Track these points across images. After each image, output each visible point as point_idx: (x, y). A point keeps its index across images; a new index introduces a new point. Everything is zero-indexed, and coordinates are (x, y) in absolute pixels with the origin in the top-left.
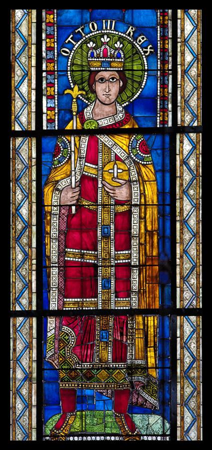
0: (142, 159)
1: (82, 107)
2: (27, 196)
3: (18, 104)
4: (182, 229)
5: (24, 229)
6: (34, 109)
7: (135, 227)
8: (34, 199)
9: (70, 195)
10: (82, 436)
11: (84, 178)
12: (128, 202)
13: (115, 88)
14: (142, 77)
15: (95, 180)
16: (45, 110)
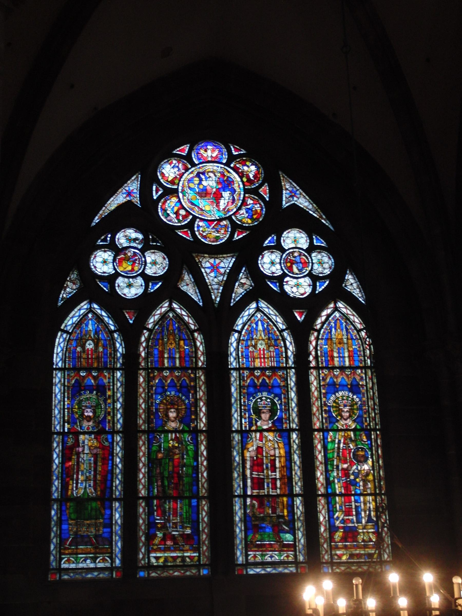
0: (279, 440)
1: (256, 422)
2: (238, 453)
3: (234, 421)
7: (278, 464)
8: (240, 454)
9: (254, 453)
12: (274, 456)
15: (262, 448)
16: (243, 423)
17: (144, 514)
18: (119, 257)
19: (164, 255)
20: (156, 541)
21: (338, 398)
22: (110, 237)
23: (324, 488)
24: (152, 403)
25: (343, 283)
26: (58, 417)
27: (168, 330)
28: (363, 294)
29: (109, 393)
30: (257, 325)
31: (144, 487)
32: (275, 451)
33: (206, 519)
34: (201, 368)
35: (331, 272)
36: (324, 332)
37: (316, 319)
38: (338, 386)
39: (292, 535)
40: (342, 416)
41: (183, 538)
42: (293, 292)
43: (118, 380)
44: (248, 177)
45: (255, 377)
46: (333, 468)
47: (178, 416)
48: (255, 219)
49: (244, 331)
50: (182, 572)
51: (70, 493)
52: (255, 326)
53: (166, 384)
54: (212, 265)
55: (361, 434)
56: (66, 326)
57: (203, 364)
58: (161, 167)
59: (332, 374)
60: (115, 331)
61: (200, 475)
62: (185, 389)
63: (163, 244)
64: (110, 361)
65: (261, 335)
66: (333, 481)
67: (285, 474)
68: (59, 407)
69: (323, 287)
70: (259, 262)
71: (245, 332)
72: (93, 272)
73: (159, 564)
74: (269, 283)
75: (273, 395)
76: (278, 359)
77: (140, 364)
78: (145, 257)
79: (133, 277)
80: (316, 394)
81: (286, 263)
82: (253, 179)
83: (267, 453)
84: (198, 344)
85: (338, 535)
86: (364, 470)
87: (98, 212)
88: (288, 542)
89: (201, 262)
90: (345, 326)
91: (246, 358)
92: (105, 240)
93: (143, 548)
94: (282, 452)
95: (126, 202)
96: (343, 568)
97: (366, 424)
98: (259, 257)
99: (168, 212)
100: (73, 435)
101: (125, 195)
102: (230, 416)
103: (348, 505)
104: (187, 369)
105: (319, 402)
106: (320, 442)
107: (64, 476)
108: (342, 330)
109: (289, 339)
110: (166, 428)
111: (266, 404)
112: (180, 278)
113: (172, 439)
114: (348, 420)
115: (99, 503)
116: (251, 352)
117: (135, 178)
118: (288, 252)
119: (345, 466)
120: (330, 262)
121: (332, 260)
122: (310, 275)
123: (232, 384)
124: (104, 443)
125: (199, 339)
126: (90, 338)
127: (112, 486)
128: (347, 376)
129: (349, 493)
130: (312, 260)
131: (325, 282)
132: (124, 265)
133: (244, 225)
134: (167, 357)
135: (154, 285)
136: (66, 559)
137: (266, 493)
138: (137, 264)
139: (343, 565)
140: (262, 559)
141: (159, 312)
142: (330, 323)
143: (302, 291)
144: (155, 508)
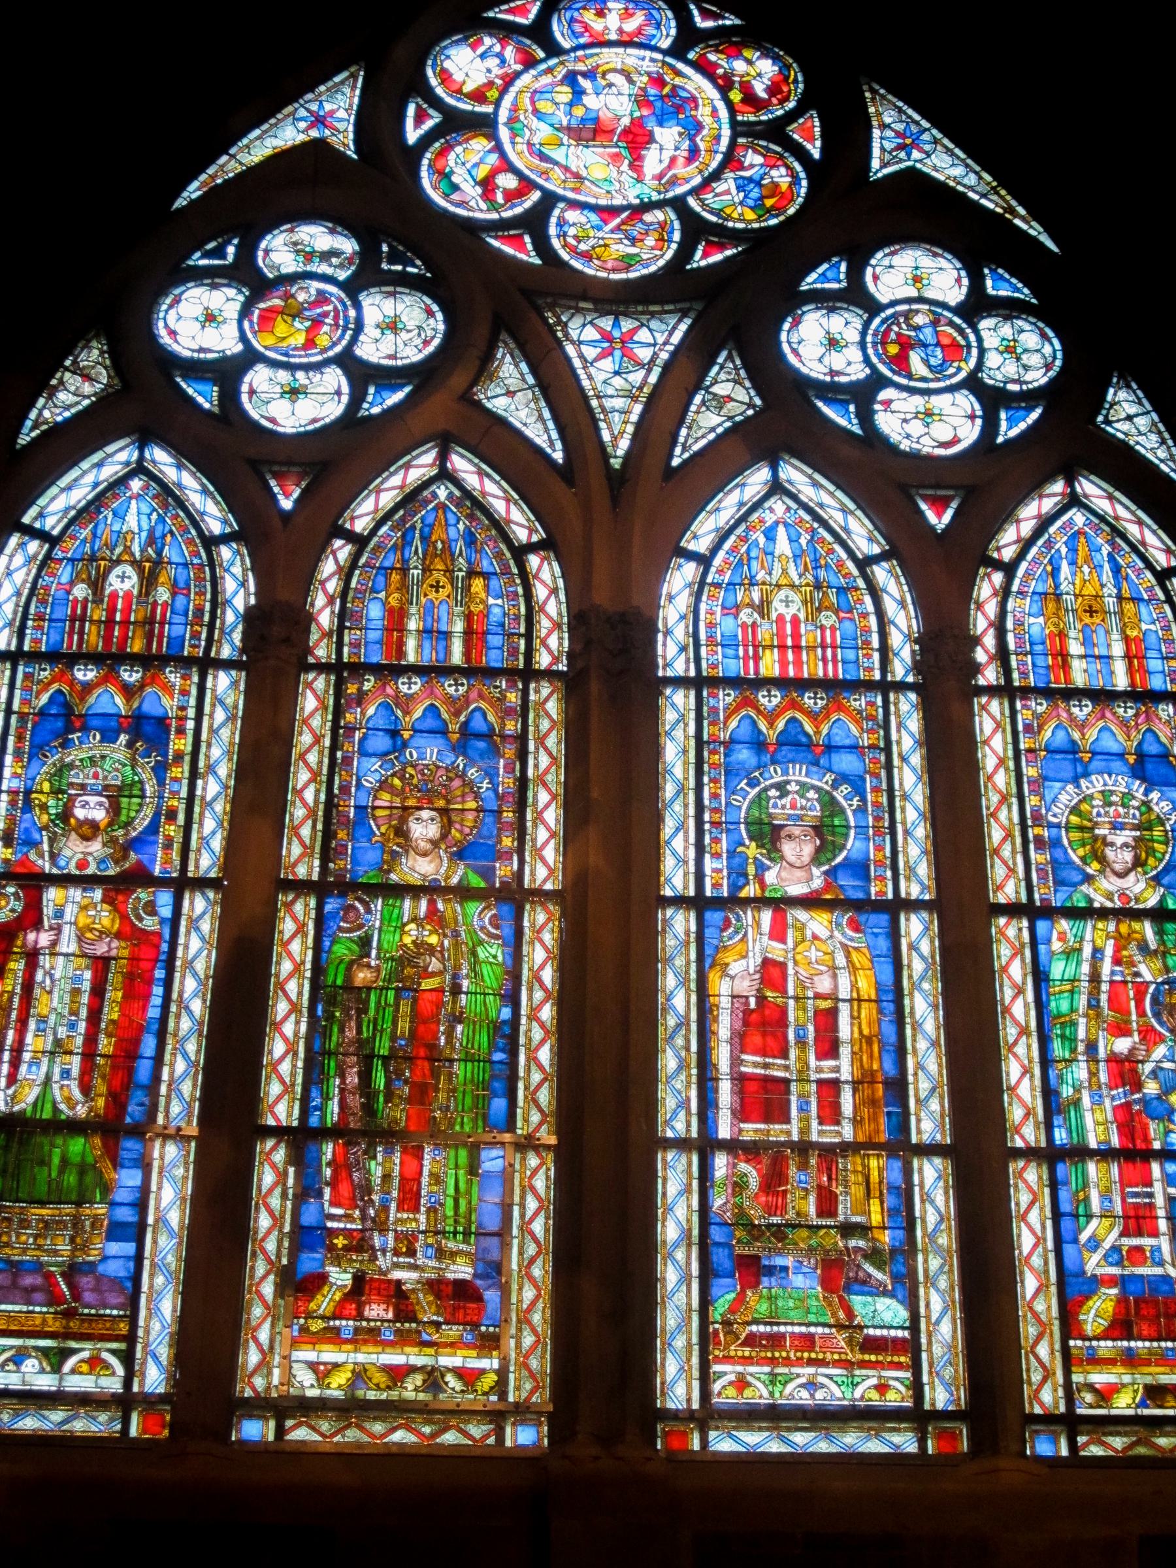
0: (852, 940)
1: (761, 869)
2: (685, 982)
3: (668, 863)
4: (914, 1036)
5: (678, 1026)
6: (692, 868)
7: (845, 1030)
8: (693, 986)
9: (746, 983)
10: (771, 1324)
11: (767, 963)
13: (808, 850)
14: (846, 836)
15: (783, 966)
16: (708, 870)
17: (278, 1191)
18: (262, 305)
19: (428, 301)
20: (324, 1302)
21: (1091, 797)
22: (237, 247)
23: (1037, 1125)
24: (345, 789)
25: (1099, 413)
27: (424, 539)
29: (183, 744)
30: (770, 535)
31: (288, 1089)
33: (538, 1227)
34: (549, 674)
35: (1052, 381)
36: (1027, 573)
39: (901, 1302)
41: (438, 1296)
42: (908, 436)
43: (218, 700)
44: (747, 89)
45: (759, 712)
46: (1073, 1050)
47: (444, 835)
48: (768, 211)
50: (427, 1430)
52: (762, 540)
53: (407, 721)
56: (41, 515)
57: (556, 660)
58: (441, 52)
59: (1064, 715)
60: (225, 539)
61: (522, 1058)
62: (482, 744)
63: (428, 270)
64: (196, 635)
65: (785, 572)
66: (1077, 1103)
67: (875, 1067)
69: (1023, 426)
70: (783, 336)
72: (162, 349)
73: (328, 1392)
74: (820, 404)
75: (829, 777)
76: (850, 655)
77: (309, 651)
78: (358, 306)
79: (307, 368)
80: (1000, 779)
81: (884, 343)
82: (764, 95)
83: (801, 984)
84: (541, 592)
87: (203, 171)
88: (885, 1332)
89: (565, 326)
90: (1109, 554)
92: (219, 252)
93: (267, 1326)
94: (866, 987)
95: (304, 144)
96: (1118, 1442)
98: (783, 320)
99: (455, 179)
100: (21, 887)
101: (303, 125)
103: (1136, 1195)
104: (492, 673)
105: (1015, 808)
106: (1018, 952)
108: (1098, 568)
109: (892, 588)
110: (393, 876)
111: (802, 808)
112: (484, 369)
113: (414, 919)
114: (1132, 877)
115: (98, 1141)
116: (744, 626)
117: (347, 79)
118: (889, 311)
119: (1122, 1045)
120: (1047, 350)
121: (1056, 342)
122: (973, 384)
123: (667, 734)
124: (141, 919)
125: (545, 575)
126: (126, 557)
127: (156, 1078)
128: (1124, 723)
129: (1140, 1145)
130: (980, 340)
131: (1030, 409)
132: (281, 328)
133: (730, 224)
134: (418, 631)
135: (385, 394)
138: (326, 328)
139: (1121, 1429)
140: (771, 1394)
141: (396, 480)
142: (1049, 544)
143: (943, 432)
144: (328, 1172)
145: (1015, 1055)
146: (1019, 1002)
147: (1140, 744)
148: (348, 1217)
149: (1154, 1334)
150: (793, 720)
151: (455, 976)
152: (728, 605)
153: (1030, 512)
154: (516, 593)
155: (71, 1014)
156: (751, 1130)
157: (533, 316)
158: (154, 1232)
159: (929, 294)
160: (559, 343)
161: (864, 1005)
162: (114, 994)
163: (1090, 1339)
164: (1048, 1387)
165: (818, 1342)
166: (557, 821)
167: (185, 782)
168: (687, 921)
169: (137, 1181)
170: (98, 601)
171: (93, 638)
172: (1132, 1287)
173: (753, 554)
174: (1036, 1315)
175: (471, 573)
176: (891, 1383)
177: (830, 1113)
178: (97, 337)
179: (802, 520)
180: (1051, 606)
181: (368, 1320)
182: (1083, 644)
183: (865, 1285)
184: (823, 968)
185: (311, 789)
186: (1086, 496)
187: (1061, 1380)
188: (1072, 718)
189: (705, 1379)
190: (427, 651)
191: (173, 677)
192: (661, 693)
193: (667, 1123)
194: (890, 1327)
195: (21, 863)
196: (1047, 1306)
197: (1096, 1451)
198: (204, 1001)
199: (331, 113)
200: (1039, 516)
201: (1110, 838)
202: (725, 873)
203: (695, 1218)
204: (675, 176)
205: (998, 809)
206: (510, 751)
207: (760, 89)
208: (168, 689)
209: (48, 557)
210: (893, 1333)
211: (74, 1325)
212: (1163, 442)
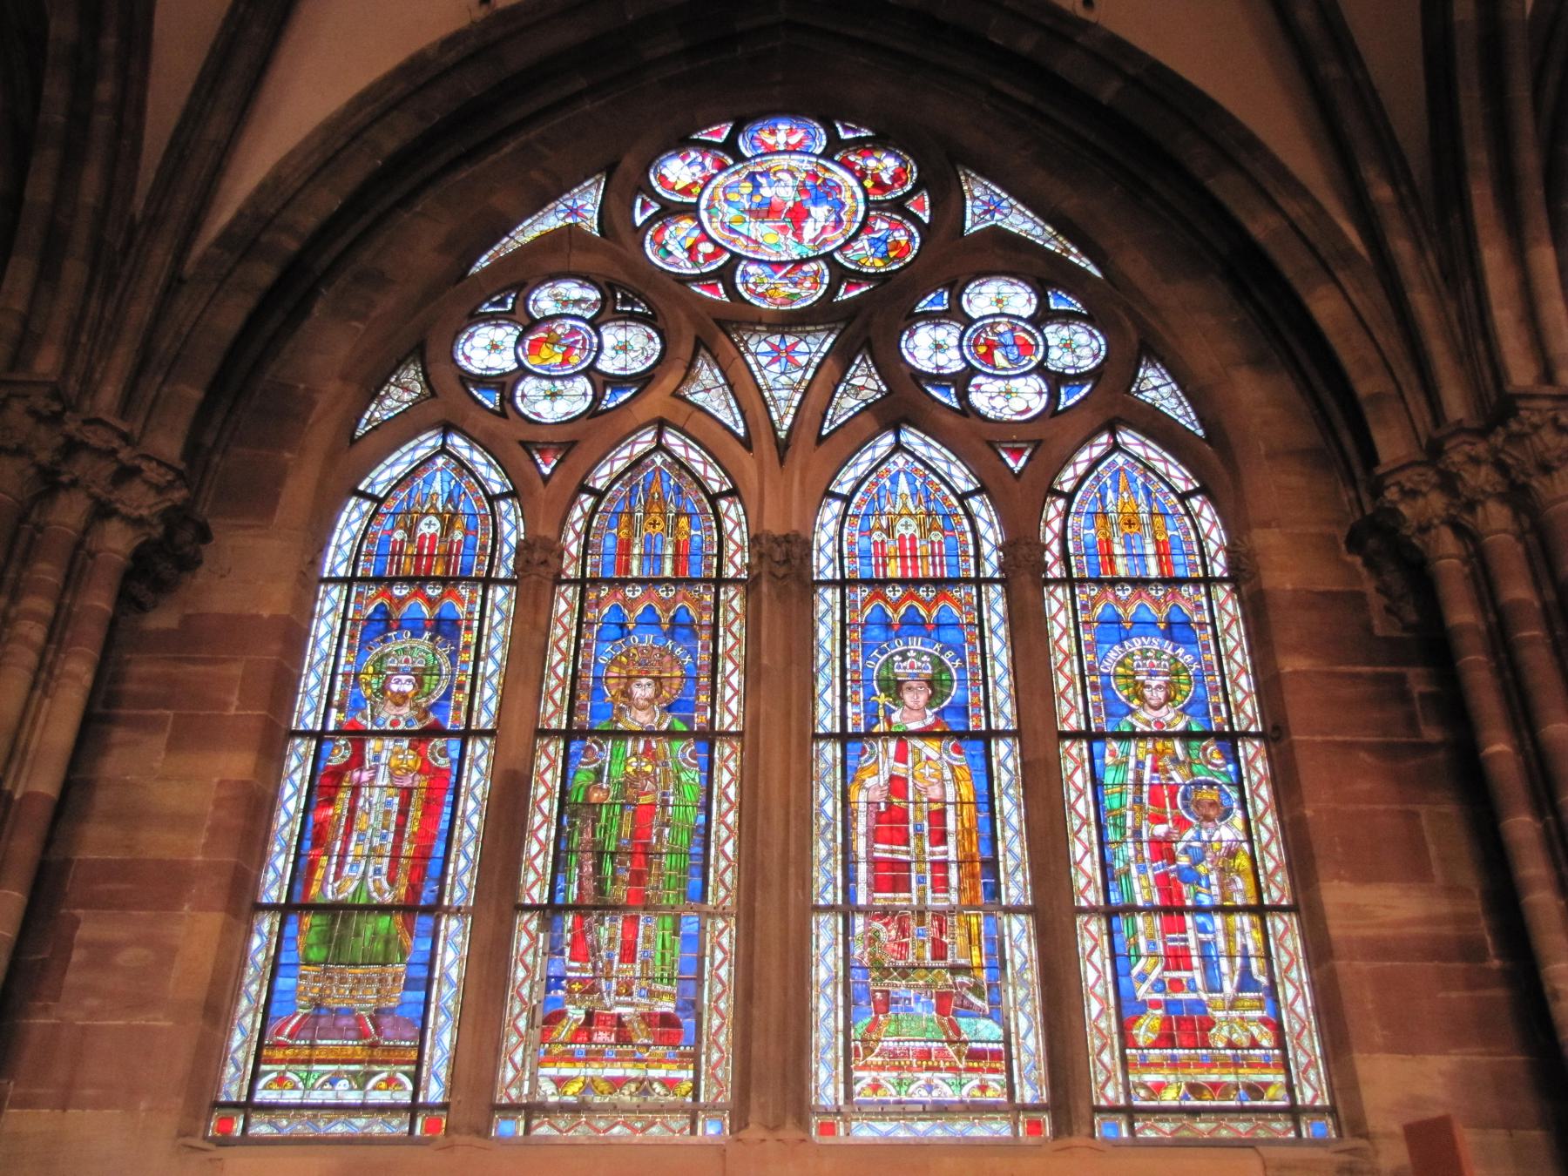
1: (889, 712)
3: (821, 710)
5: (828, 825)
6: (838, 713)
7: (951, 824)
8: (839, 796)
9: (878, 793)
11: (893, 778)
13: (923, 698)
15: (905, 780)
17: (531, 951)
18: (532, 338)
19: (650, 330)
20: (563, 1031)
21: (1132, 654)
26: (316, 693)
28: (1189, 409)
30: (894, 480)
32: (943, 787)
33: (723, 972)
34: (734, 581)
36: (1082, 501)
37: (1061, 468)
38: (1128, 626)
40: (1142, 698)
41: (649, 1025)
42: (994, 408)
43: (496, 606)
45: (886, 602)
46: (1123, 835)
47: (657, 696)
48: (892, 260)
49: (858, 495)
51: (315, 889)
52: (888, 484)
54: (775, 348)
55: (1205, 749)
56: (372, 484)
57: (739, 571)
59: (1111, 597)
60: (503, 496)
62: (686, 631)
63: (649, 309)
64: (481, 563)
65: (905, 505)
66: (1127, 873)
68: (320, 670)
69: (1077, 397)
70: (903, 344)
71: (862, 500)
73: (565, 1098)
76: (953, 560)
77: (561, 571)
78: (599, 334)
79: (562, 378)
81: (975, 345)
82: (889, 182)
84: (729, 525)
85: (1146, 1028)
86: (1221, 841)
89: (746, 343)
91: (861, 557)
92: (502, 303)
93: (520, 1050)
97: (1218, 720)
98: (902, 333)
99: (669, 248)
100: (350, 740)
101: (561, 215)
102: (809, 696)
104: (691, 582)
105: (1076, 663)
107: (307, 844)
109: (984, 513)
113: (634, 754)
114: (1164, 709)
115: (399, 918)
116: (876, 543)
118: (979, 324)
119: (1160, 830)
120: (1095, 344)
122: (1041, 370)
123: (820, 620)
125: (732, 513)
127: (444, 873)
128: (1155, 601)
130: (1045, 340)
131: (1082, 386)
132: (545, 352)
133: (865, 270)
136: (274, 1075)
137: (915, 902)
138: (577, 351)
140: (899, 1093)
141: (626, 453)
142: (1098, 478)
144: (569, 937)
145: (1079, 839)
146: (1082, 801)
147: (1168, 615)
148: (584, 969)
149: (1193, 1045)
150: (911, 607)
151: (664, 794)
152: (864, 529)
153: (1083, 458)
154: (711, 527)
155: (383, 828)
156: (882, 898)
157: (722, 337)
158: (439, 983)
159: (1008, 311)
160: (742, 354)
161: (965, 806)
162: (415, 813)
163: (1142, 1049)
164: (1110, 1086)
165: (934, 1053)
166: (739, 683)
167: (471, 664)
168: (834, 750)
169: (428, 947)
170: (411, 541)
171: (407, 566)
172: (1172, 1008)
173: (882, 494)
174: (1099, 1030)
175: (678, 515)
176: (990, 1083)
177: (941, 884)
178: (414, 362)
179: (917, 469)
180: (1100, 521)
181: (596, 1044)
182: (1124, 547)
183: (969, 1011)
184: (935, 780)
185: (562, 665)
186: (1125, 444)
187: (1120, 1080)
188: (1117, 598)
189: (849, 1082)
190: (646, 569)
191: (464, 592)
192: (816, 592)
193: (818, 895)
194: (988, 1042)
195: (351, 724)
196: (1109, 1024)
197: (1150, 1134)
198: (481, 815)
199: (582, 206)
200: (1090, 460)
201: (1147, 682)
202: (862, 715)
203: (840, 963)
204: (825, 239)
205: (1063, 664)
206: (705, 635)
207: (886, 178)
208: (460, 600)
209: (376, 511)
210: (990, 1046)
211: (377, 1053)
212: (1181, 403)
